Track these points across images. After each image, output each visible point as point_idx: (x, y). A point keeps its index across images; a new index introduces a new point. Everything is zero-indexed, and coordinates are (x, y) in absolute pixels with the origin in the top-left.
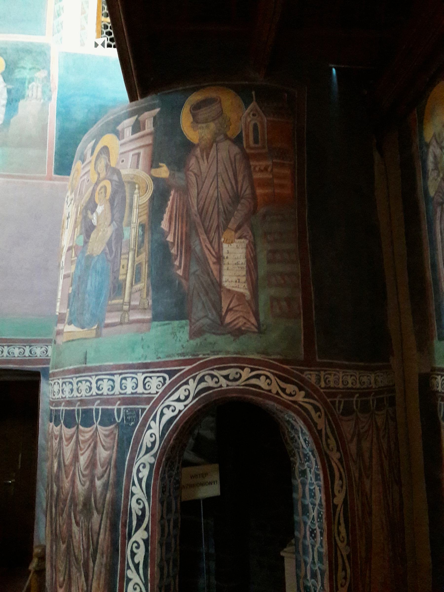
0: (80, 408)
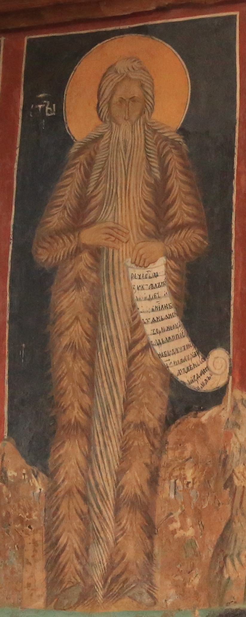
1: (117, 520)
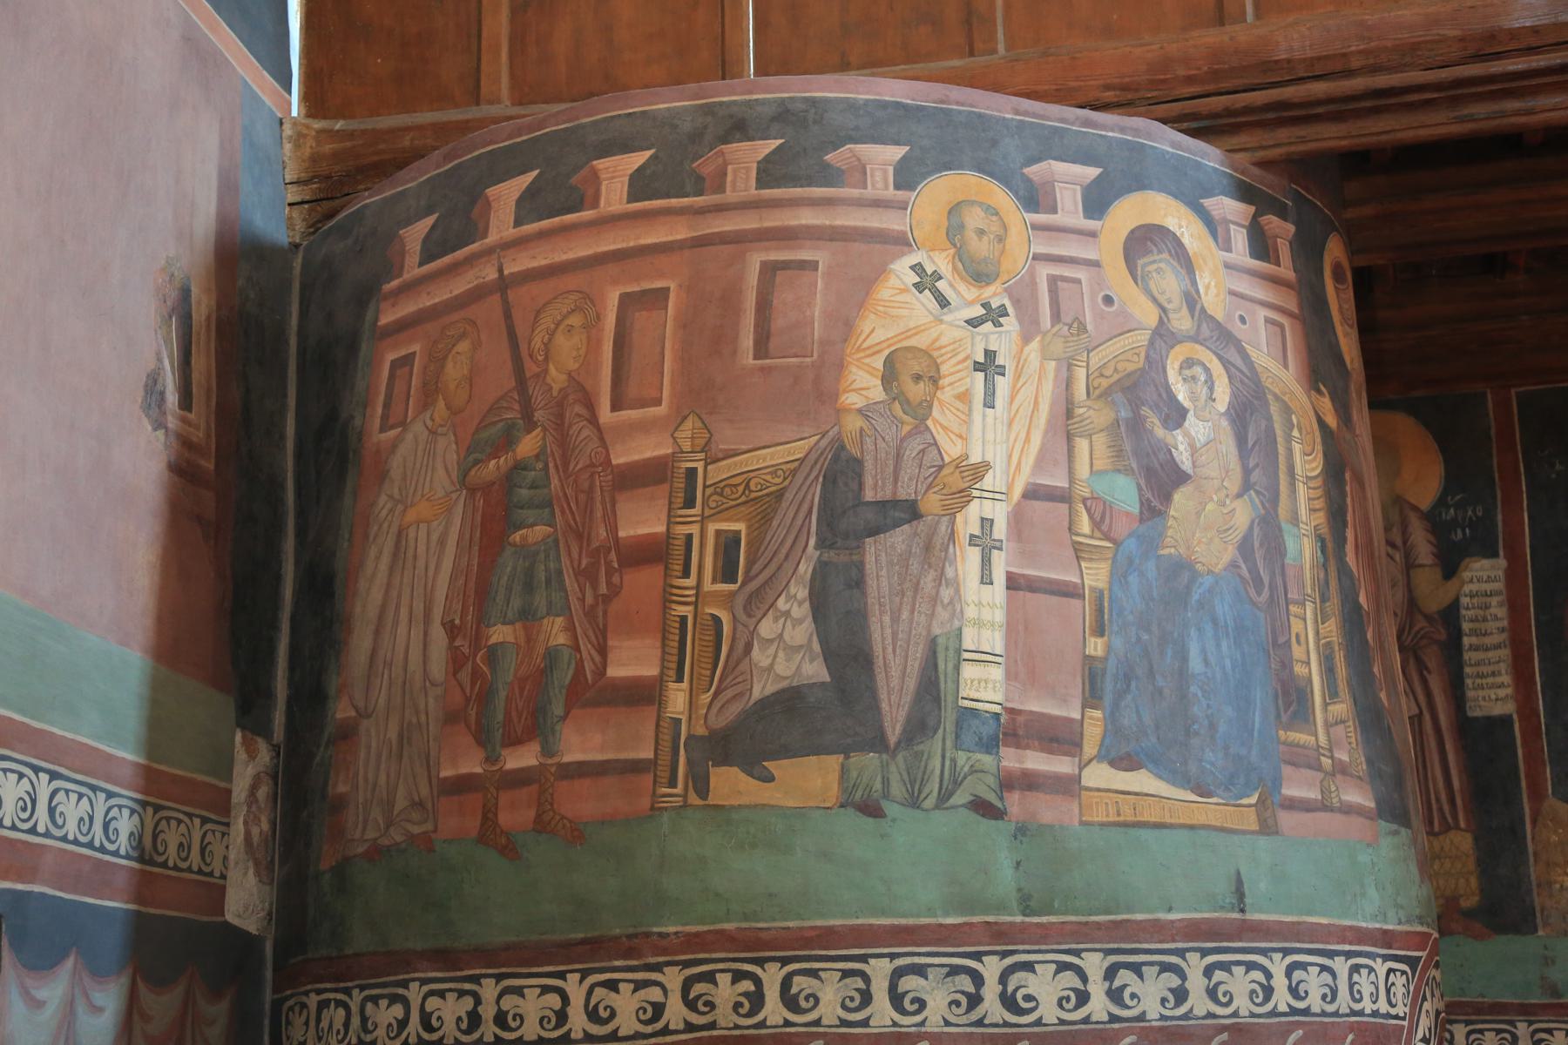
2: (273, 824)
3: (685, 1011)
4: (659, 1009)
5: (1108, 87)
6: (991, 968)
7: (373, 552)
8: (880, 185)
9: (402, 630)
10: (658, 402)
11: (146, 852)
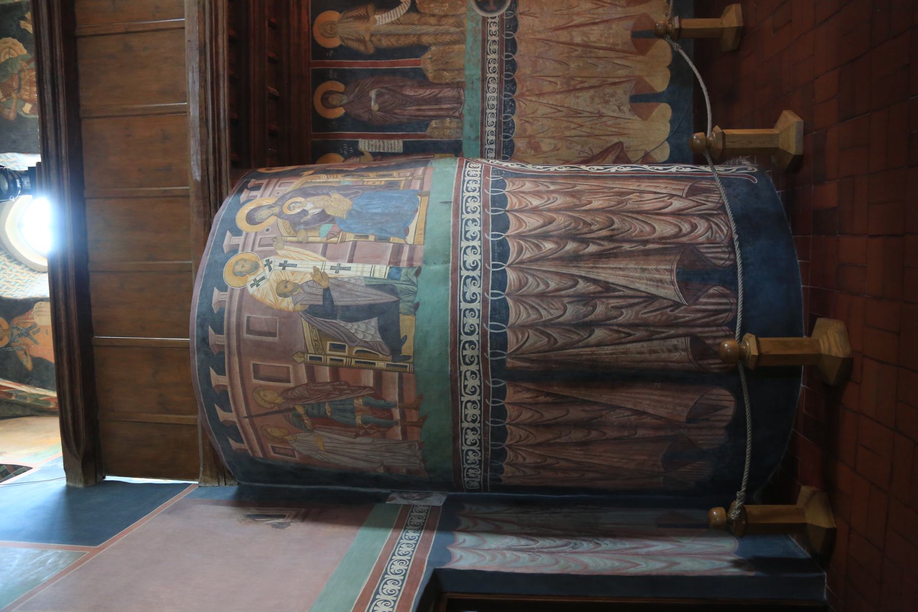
0: (491, 208)
1: (443, 25)
2: (415, 493)
3: (474, 365)
4: (473, 373)
5: (204, 230)
6: (465, 273)
7: (333, 460)
8: (225, 296)
9: (357, 451)
10: (288, 368)
11: (419, 528)
